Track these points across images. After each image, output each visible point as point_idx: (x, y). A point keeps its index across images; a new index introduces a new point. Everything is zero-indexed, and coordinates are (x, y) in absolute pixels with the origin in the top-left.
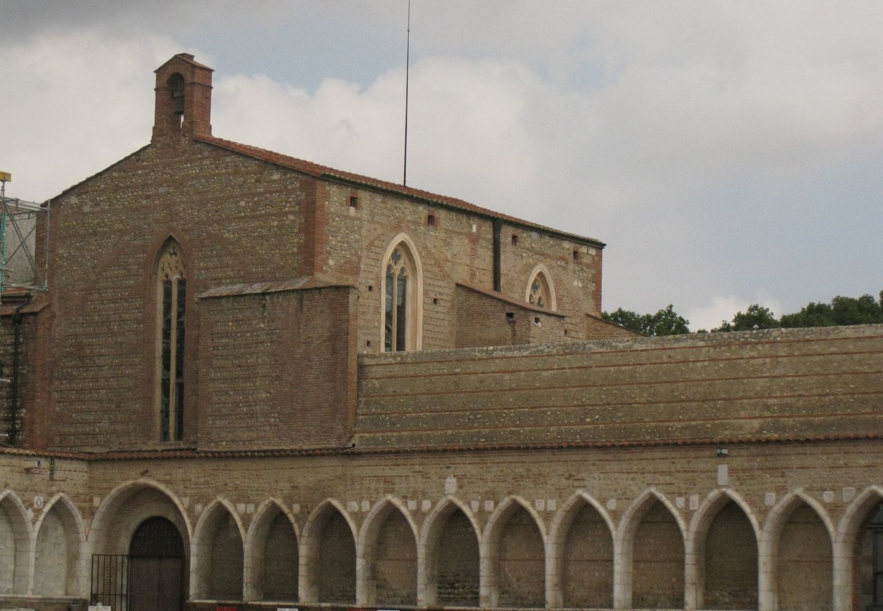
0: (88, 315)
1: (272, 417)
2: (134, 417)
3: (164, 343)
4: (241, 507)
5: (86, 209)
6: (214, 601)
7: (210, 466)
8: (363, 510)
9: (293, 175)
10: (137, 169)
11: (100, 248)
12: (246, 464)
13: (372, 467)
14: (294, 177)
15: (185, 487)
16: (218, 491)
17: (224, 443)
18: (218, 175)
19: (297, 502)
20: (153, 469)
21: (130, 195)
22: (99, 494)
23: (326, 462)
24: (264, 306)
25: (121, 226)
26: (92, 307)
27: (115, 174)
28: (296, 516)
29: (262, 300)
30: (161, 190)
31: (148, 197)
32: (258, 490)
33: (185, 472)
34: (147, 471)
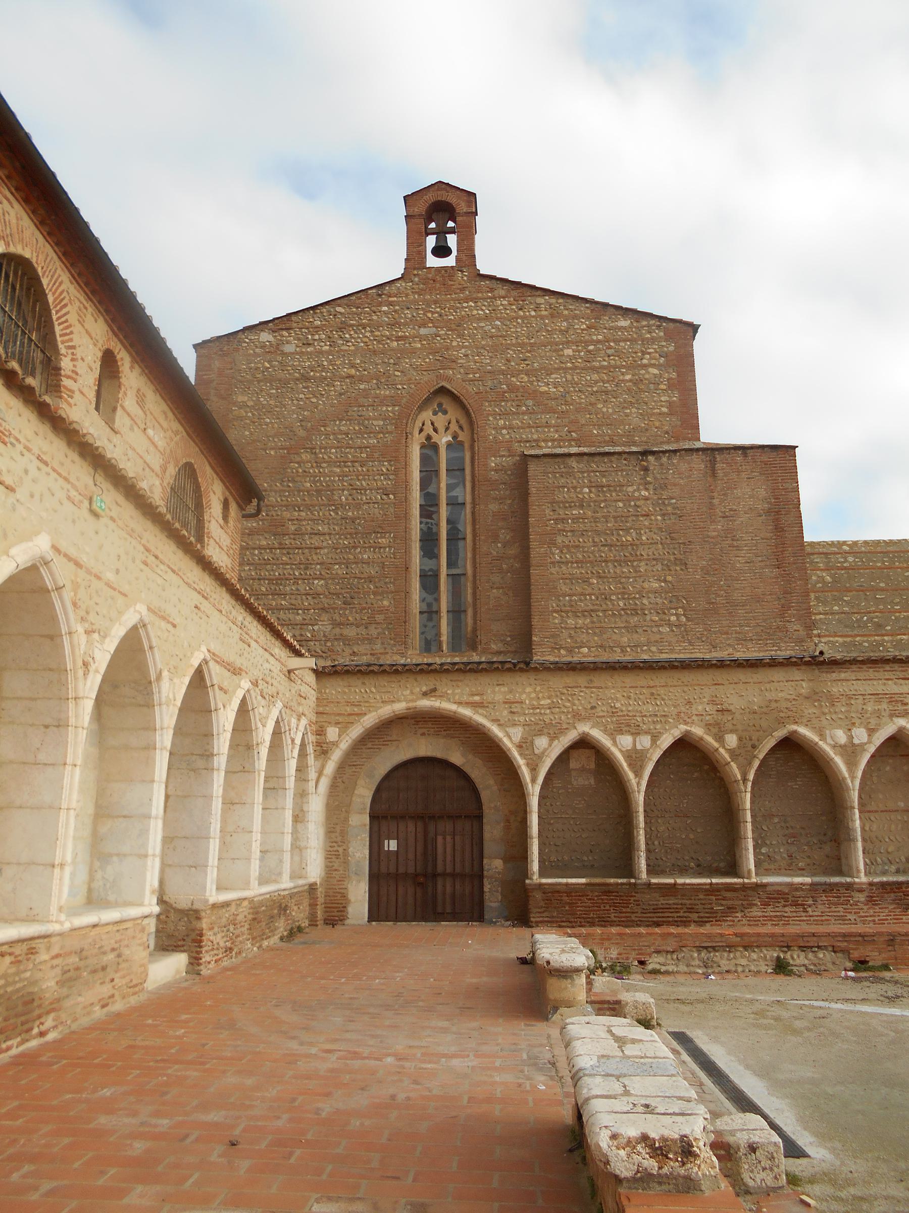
0: (294, 481)
1: (673, 615)
2: (380, 618)
3: (421, 523)
4: (626, 741)
5: (289, 348)
6: (583, 881)
7: (558, 682)
8: (856, 741)
9: (652, 322)
10: (380, 304)
11: (315, 397)
12: (629, 679)
13: (864, 682)
14: (653, 325)
15: (512, 712)
16: (578, 717)
17: (585, 650)
18: (522, 318)
19: (732, 731)
20: (445, 685)
21: (368, 334)
22: (337, 723)
23: (777, 675)
24: (646, 469)
25: (353, 371)
26: (300, 470)
27: (339, 309)
28: (731, 752)
29: (642, 460)
30: (423, 331)
31: (398, 339)
32: (656, 715)
33: (511, 692)
34: (435, 690)
